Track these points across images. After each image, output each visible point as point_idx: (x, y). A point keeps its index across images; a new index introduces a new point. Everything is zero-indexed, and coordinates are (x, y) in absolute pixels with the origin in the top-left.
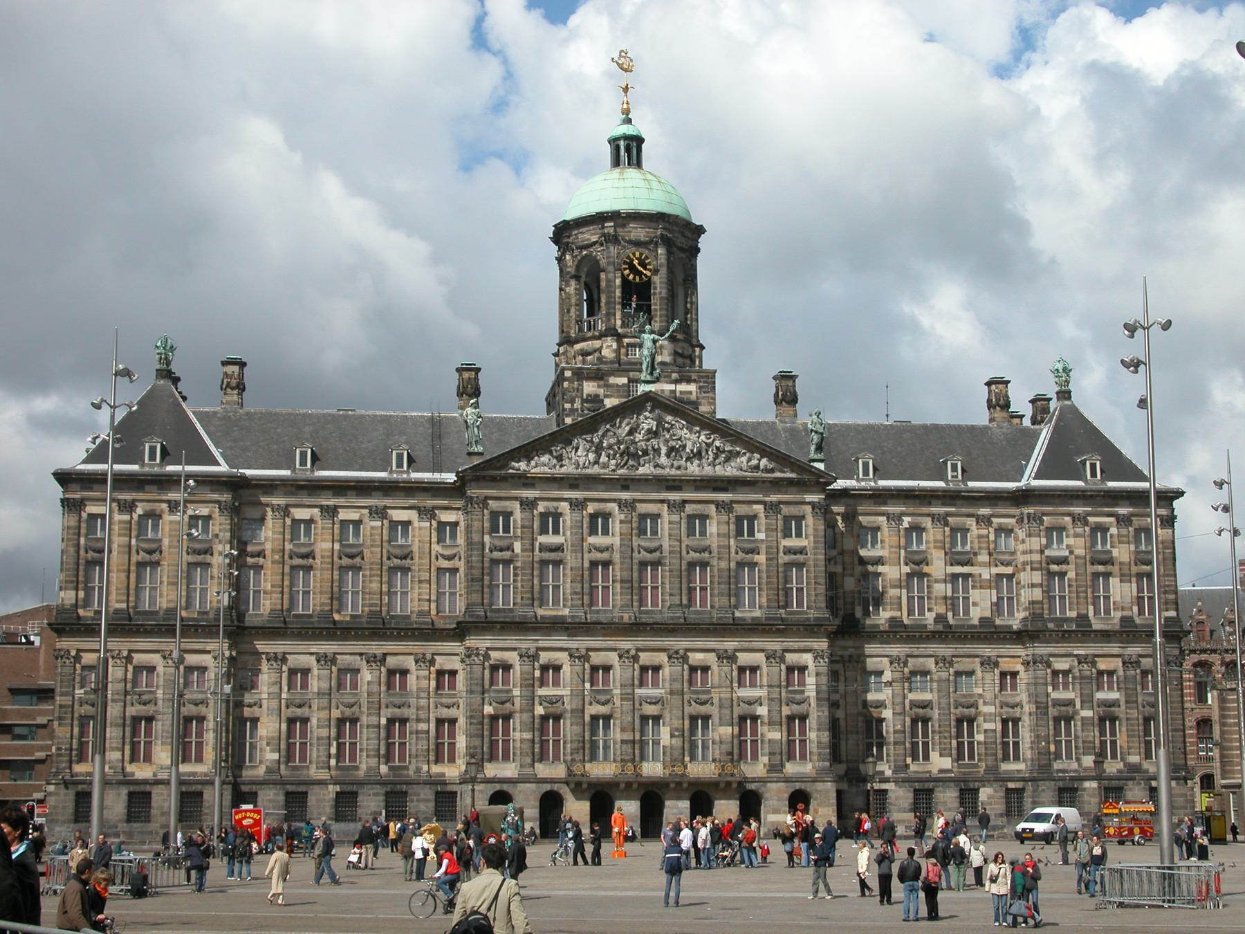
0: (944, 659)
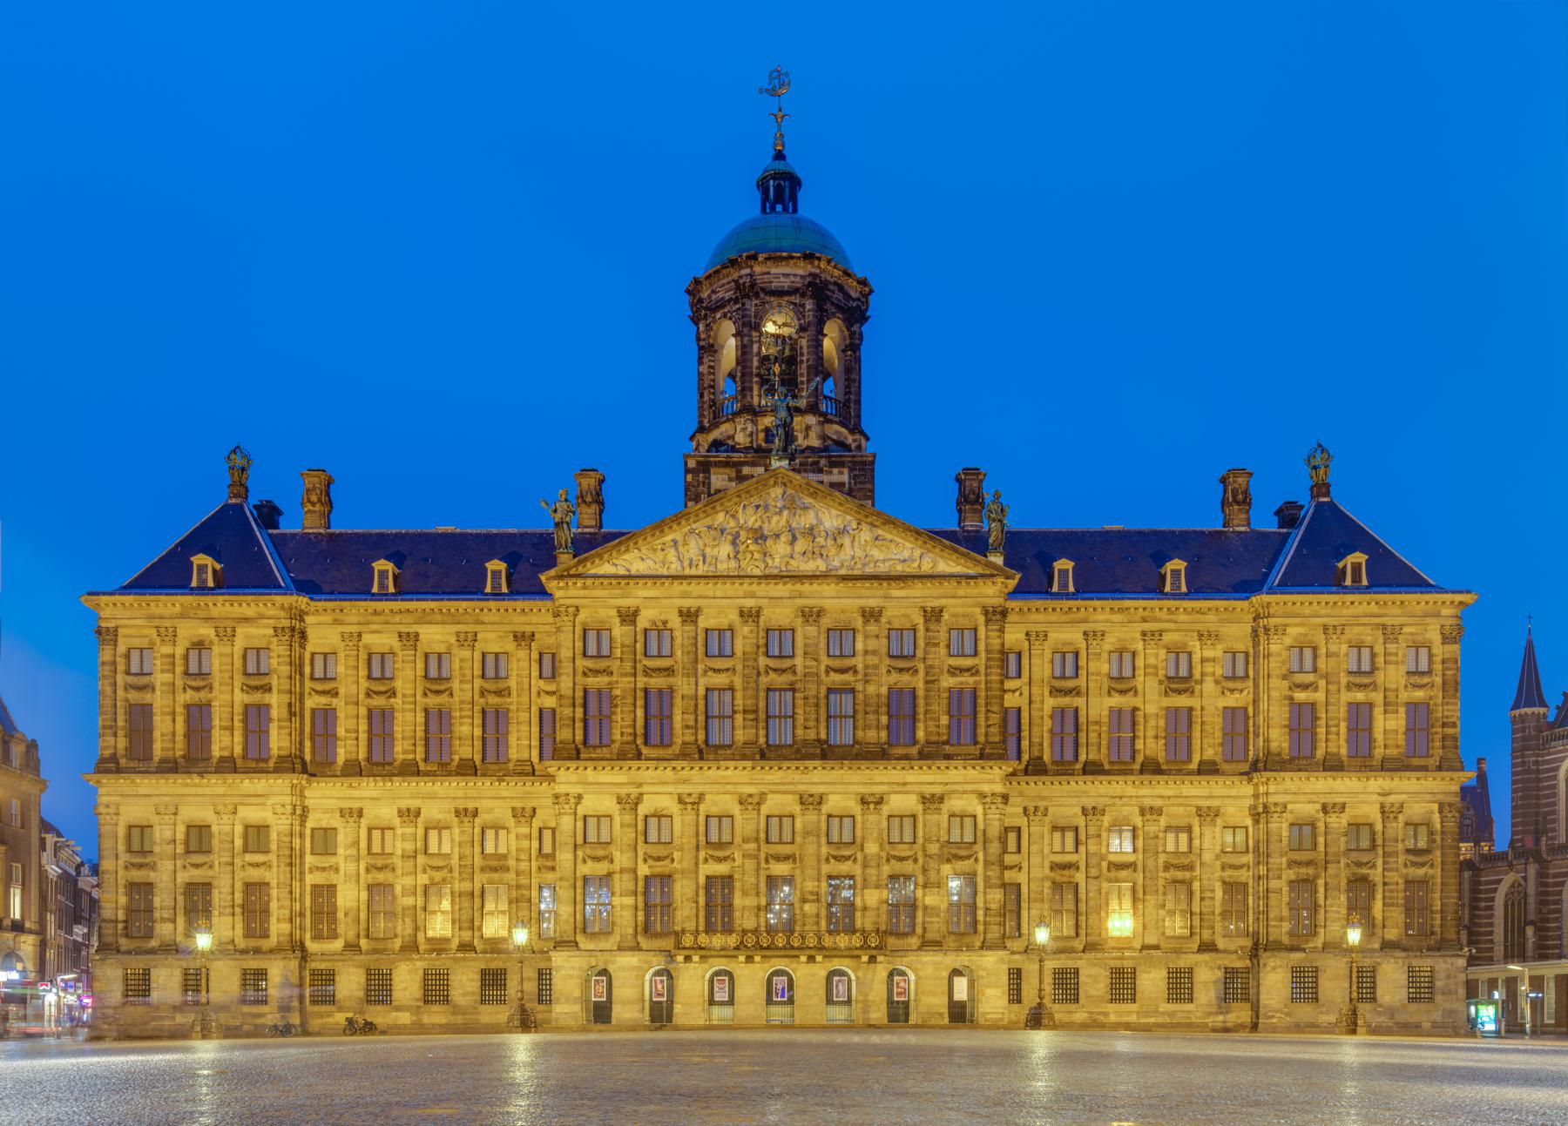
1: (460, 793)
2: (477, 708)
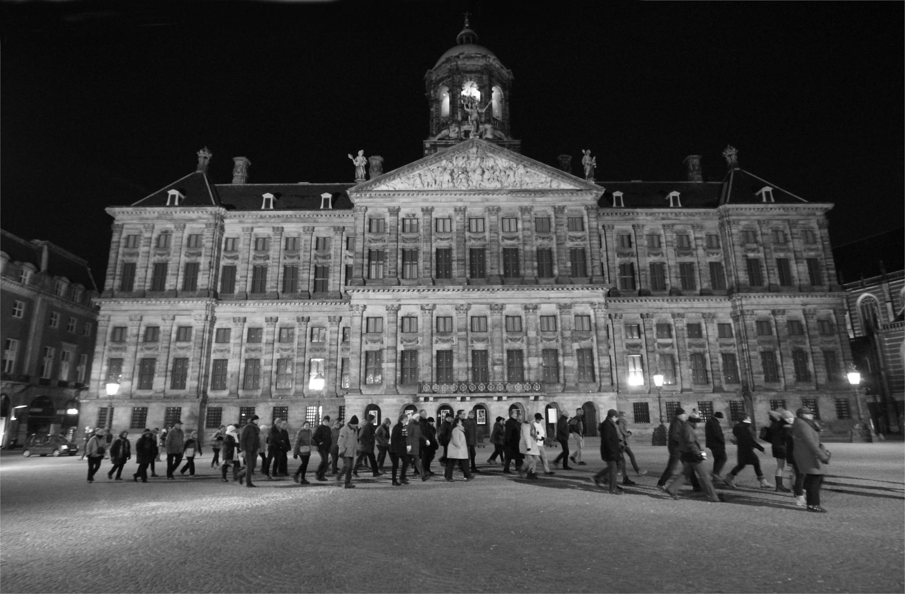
0: (679, 315)
1: (301, 309)
2: (312, 265)
